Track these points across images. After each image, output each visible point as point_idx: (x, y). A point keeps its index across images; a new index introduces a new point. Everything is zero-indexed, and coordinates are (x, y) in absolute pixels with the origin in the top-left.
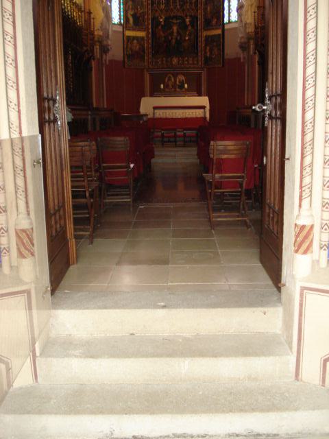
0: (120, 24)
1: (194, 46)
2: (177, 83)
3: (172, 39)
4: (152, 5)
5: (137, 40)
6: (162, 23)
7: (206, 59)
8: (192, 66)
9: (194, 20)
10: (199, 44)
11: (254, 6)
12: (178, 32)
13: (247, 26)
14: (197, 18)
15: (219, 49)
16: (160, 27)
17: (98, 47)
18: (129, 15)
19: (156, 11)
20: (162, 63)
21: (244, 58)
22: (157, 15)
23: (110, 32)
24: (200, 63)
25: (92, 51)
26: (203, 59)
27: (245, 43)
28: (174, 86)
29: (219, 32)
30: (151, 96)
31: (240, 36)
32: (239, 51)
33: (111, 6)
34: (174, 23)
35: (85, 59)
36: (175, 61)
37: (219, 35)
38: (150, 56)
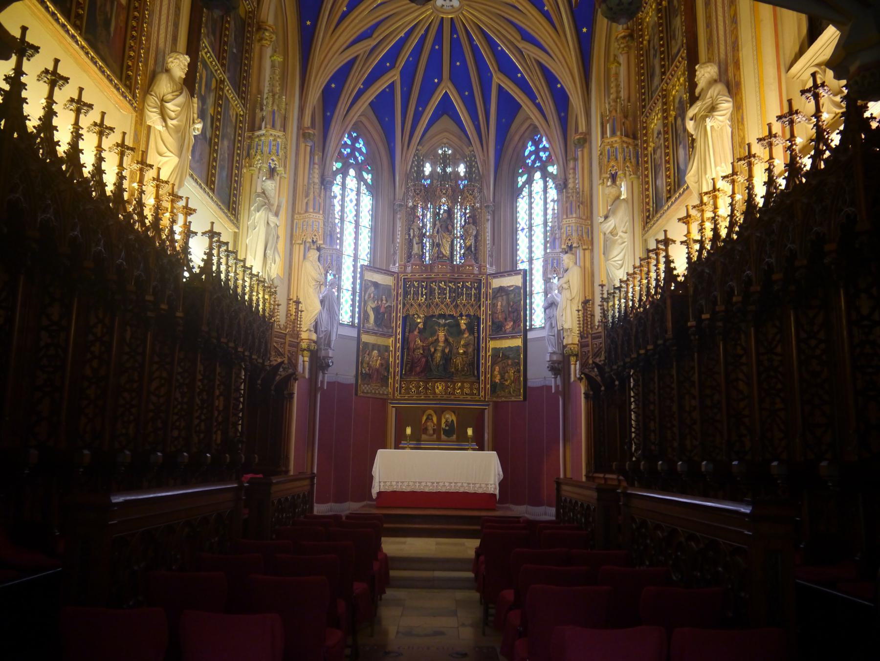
0: (352, 325)
1: (473, 365)
2: (443, 426)
4: (404, 298)
5: (379, 351)
6: (420, 326)
7: (494, 386)
8: (469, 397)
9: (474, 323)
10: (482, 361)
11: (576, 301)
12: (446, 340)
13: (565, 334)
14: (478, 319)
15: (519, 371)
16: (416, 333)
17: (307, 359)
19: (412, 305)
20: (419, 393)
21: (557, 387)
22: (411, 312)
23: (334, 337)
24: (482, 394)
25: (295, 366)
26: (488, 386)
27: (559, 362)
28: (437, 430)
29: (518, 342)
30: (397, 447)
31: (550, 350)
32: (550, 375)
33: (339, 297)
34: (439, 324)
35: (278, 378)
36: (440, 388)
38: (398, 378)
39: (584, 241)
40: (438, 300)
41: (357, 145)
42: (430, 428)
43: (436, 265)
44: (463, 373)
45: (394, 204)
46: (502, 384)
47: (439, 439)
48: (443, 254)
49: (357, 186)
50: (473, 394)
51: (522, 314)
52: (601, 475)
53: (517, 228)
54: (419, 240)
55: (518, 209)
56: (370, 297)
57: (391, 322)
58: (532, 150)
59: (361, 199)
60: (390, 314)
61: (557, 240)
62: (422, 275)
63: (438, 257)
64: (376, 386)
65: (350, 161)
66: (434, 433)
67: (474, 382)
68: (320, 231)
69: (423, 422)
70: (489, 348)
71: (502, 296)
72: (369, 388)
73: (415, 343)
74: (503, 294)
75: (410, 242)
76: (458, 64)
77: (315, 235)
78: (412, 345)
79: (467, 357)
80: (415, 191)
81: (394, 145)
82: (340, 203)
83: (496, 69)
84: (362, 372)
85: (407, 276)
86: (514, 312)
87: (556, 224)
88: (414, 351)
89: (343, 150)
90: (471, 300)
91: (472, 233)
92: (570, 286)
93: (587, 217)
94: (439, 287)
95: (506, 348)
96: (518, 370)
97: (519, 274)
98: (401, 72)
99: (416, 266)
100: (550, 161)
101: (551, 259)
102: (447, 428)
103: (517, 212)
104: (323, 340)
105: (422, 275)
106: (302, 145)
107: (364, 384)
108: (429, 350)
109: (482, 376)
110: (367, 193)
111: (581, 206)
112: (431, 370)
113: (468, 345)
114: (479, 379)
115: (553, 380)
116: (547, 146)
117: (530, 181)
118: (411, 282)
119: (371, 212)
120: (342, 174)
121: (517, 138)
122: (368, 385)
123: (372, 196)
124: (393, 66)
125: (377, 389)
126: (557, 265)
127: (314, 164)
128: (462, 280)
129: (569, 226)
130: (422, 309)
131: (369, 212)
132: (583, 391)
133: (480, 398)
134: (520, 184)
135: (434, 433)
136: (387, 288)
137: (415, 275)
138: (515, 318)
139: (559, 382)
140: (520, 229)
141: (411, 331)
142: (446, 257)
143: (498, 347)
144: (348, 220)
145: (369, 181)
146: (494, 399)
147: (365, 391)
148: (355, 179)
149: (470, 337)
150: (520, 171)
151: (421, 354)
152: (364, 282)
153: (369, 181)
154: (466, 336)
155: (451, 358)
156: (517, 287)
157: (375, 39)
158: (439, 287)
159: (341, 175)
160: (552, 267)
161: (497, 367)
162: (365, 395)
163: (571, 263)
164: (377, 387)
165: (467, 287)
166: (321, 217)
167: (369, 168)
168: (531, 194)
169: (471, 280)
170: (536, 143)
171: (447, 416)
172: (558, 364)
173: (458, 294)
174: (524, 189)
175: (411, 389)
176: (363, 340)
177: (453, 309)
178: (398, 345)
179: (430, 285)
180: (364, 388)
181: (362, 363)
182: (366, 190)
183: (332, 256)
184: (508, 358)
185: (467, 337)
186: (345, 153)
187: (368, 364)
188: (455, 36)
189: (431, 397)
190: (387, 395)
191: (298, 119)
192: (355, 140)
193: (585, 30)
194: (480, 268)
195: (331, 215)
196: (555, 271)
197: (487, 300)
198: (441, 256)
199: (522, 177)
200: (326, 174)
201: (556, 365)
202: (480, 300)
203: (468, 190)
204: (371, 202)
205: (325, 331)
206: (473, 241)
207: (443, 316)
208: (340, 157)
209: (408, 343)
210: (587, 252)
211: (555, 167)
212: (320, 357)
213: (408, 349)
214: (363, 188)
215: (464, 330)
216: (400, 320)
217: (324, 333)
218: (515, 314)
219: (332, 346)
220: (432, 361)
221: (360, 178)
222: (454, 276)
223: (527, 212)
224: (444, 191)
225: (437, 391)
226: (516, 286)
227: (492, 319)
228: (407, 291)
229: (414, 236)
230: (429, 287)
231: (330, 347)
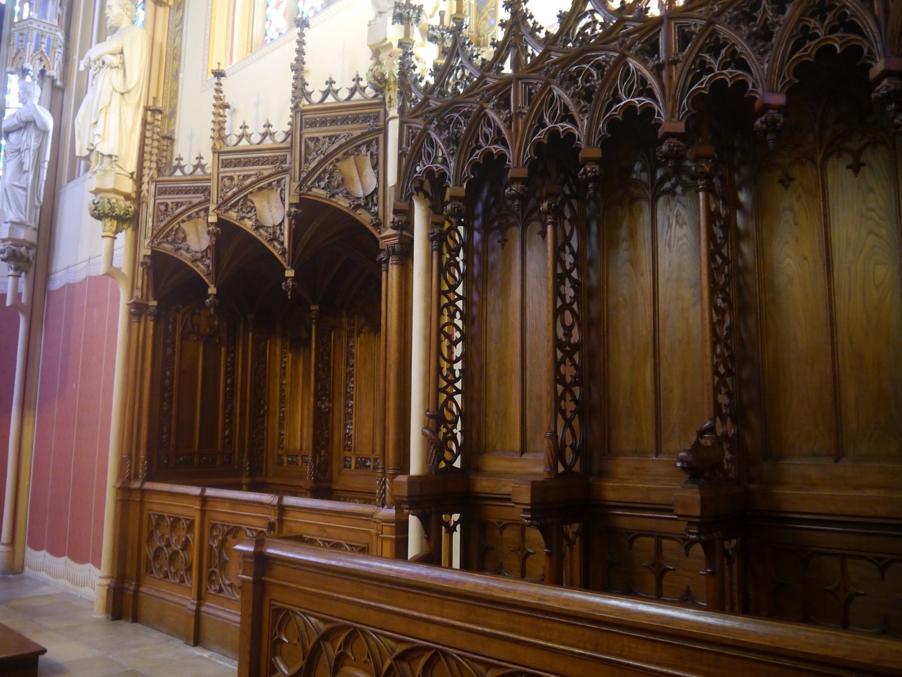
21: (17, 296)
27: (30, 246)
31: (11, 216)
52: (196, 491)
92: (123, 63)
101: (35, 33)
115: (11, 279)
126: (48, 48)
132: (124, 299)
139: (23, 287)
163: (125, 18)
172: (28, 248)
196: (41, 60)
201: (23, 250)
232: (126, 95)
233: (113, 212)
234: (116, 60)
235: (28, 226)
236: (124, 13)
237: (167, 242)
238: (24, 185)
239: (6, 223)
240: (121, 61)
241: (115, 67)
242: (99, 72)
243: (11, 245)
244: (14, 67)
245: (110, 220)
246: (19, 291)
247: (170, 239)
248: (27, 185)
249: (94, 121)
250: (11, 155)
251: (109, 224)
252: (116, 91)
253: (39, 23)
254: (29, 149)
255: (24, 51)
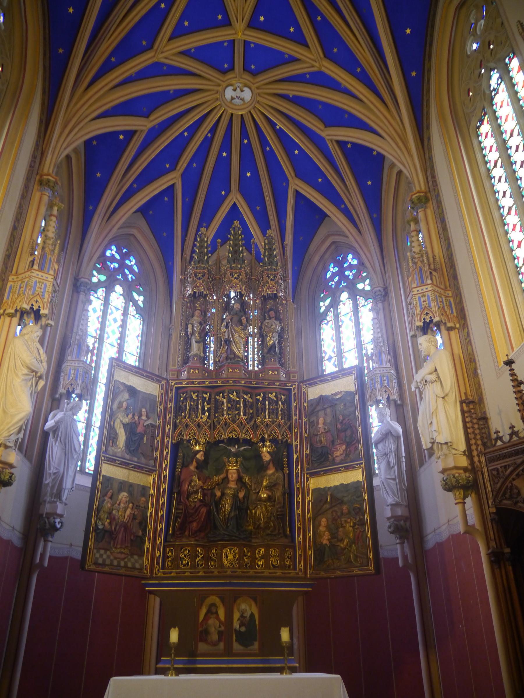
2: (236, 625)
3: (223, 494)
4: (176, 416)
5: (130, 493)
7: (320, 551)
8: (279, 573)
10: (298, 511)
12: (240, 480)
14: (289, 446)
15: (362, 523)
16: (192, 468)
18: (118, 423)
19: (187, 426)
20: (195, 566)
21: (405, 557)
23: (68, 484)
24: (300, 566)
26: (310, 552)
27: (406, 519)
31: (390, 500)
37: (357, 485)
38: (160, 540)
39: (448, 316)
40: (227, 417)
41: (127, 262)
42: (212, 630)
43: (225, 368)
44: (269, 532)
45: (170, 329)
46: (333, 546)
47: (228, 652)
48: (234, 354)
49: (124, 305)
50: (283, 567)
51: (359, 429)
53: (322, 357)
54: (200, 337)
55: (322, 337)
56: (122, 407)
57: (152, 450)
58: (334, 271)
59: (129, 320)
60: (153, 437)
61: (383, 354)
62: (204, 383)
63: (227, 358)
64: (122, 553)
65: (118, 277)
66: (220, 640)
67: (286, 546)
68: (46, 296)
69: (201, 618)
70: (308, 489)
71: (325, 409)
72: (108, 557)
73: (190, 483)
74: (326, 406)
75: (188, 342)
76: (248, 174)
77: (37, 302)
78: (185, 487)
79: (274, 506)
80: (196, 275)
81: (173, 264)
82: (100, 320)
83: (293, 174)
84: (96, 529)
85: (181, 383)
86: (345, 431)
87: (380, 335)
88: (189, 495)
89: (109, 263)
90: (277, 418)
91: (275, 328)
93: (446, 288)
94: (229, 400)
95: (336, 487)
96: (360, 519)
97: (350, 373)
98: (183, 175)
99: (195, 370)
100: (358, 278)
101: (379, 376)
102: (243, 629)
103: (321, 340)
104: (49, 489)
105: (204, 383)
106: (36, 195)
107: (98, 549)
108: (214, 495)
109: (299, 536)
110: (137, 316)
111: (434, 273)
112: (215, 527)
113: (275, 485)
114: (293, 540)
115: (398, 546)
116: (355, 262)
117: (335, 304)
118: (187, 392)
119: (140, 338)
120: (106, 288)
121: (316, 259)
122: (106, 550)
123: (143, 321)
124: (173, 168)
125: (123, 559)
126: (388, 383)
127: (51, 215)
128: (264, 390)
129: (424, 296)
130: (203, 432)
131: (138, 337)
133: (297, 574)
134: (322, 309)
135: (220, 640)
136: (148, 398)
137: (193, 383)
138: (348, 440)
139: (407, 551)
140: (326, 358)
141: (185, 466)
142: (240, 358)
143: (322, 487)
144: (109, 341)
145: (141, 304)
146: (322, 574)
147: (100, 561)
148: (122, 297)
149: (277, 475)
150: (322, 295)
151: (200, 500)
152: (112, 383)
153: (141, 304)
154: (270, 472)
155: (248, 508)
156: (350, 394)
157: (152, 121)
158: (229, 400)
159: (104, 289)
160: (382, 386)
161: (324, 520)
162: (100, 569)
163: (432, 347)
164: (123, 556)
165: (271, 401)
166: (50, 278)
167: (141, 289)
168: (338, 317)
169: (277, 390)
170: (340, 264)
171: (243, 606)
172: (405, 521)
173: (257, 410)
174: (329, 313)
175: (182, 559)
176: (103, 473)
177: (251, 432)
178: (163, 486)
179: (215, 398)
180: (98, 555)
181: (98, 511)
182: (135, 312)
183: (76, 370)
184: (342, 503)
185: (273, 474)
186: (112, 266)
187: (110, 513)
188: (246, 141)
189: (216, 573)
190: (141, 569)
191: (34, 157)
192: (125, 257)
193: (414, 74)
194: (288, 373)
195: (82, 322)
196: (386, 391)
197: (300, 418)
198: (232, 356)
199: (324, 301)
200: (81, 275)
201: (402, 523)
202: (289, 418)
203: (268, 274)
204: (141, 326)
205: (55, 474)
206: (276, 339)
207: (232, 441)
208: (104, 269)
209: (180, 484)
210: (452, 333)
211: (367, 282)
212: (42, 515)
213: (179, 493)
214: (132, 310)
215: (268, 462)
216: (167, 447)
217: (53, 477)
218: (349, 433)
219: (64, 498)
220: (218, 511)
221: (128, 297)
222: (251, 383)
223: (334, 338)
224: (236, 276)
225: (225, 562)
226: (347, 392)
227: (311, 445)
228: (180, 407)
229: (193, 333)
230: (213, 400)
231: (60, 499)
232: (446, 397)
233: (459, 484)
234: (433, 377)
235: (401, 505)
236: (430, 345)
237: (507, 499)
238: (393, 477)
239: (388, 506)
240: (437, 376)
241: (434, 381)
242: (425, 389)
243: (394, 521)
244: (372, 401)
245: (458, 490)
246: (406, 554)
247: (507, 496)
248: (395, 476)
249: (429, 422)
250: (381, 458)
251: (457, 493)
252: (439, 397)
253: (379, 369)
254: (391, 451)
255: (375, 390)
